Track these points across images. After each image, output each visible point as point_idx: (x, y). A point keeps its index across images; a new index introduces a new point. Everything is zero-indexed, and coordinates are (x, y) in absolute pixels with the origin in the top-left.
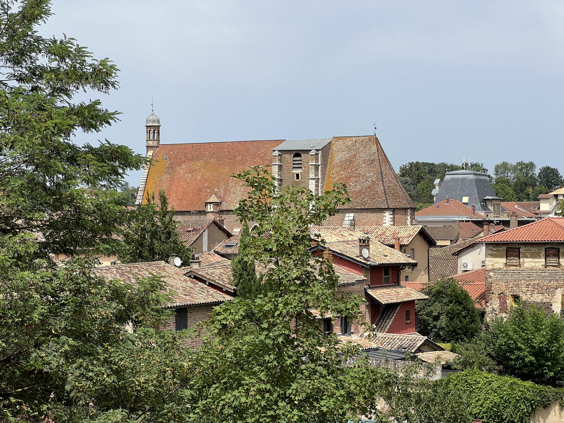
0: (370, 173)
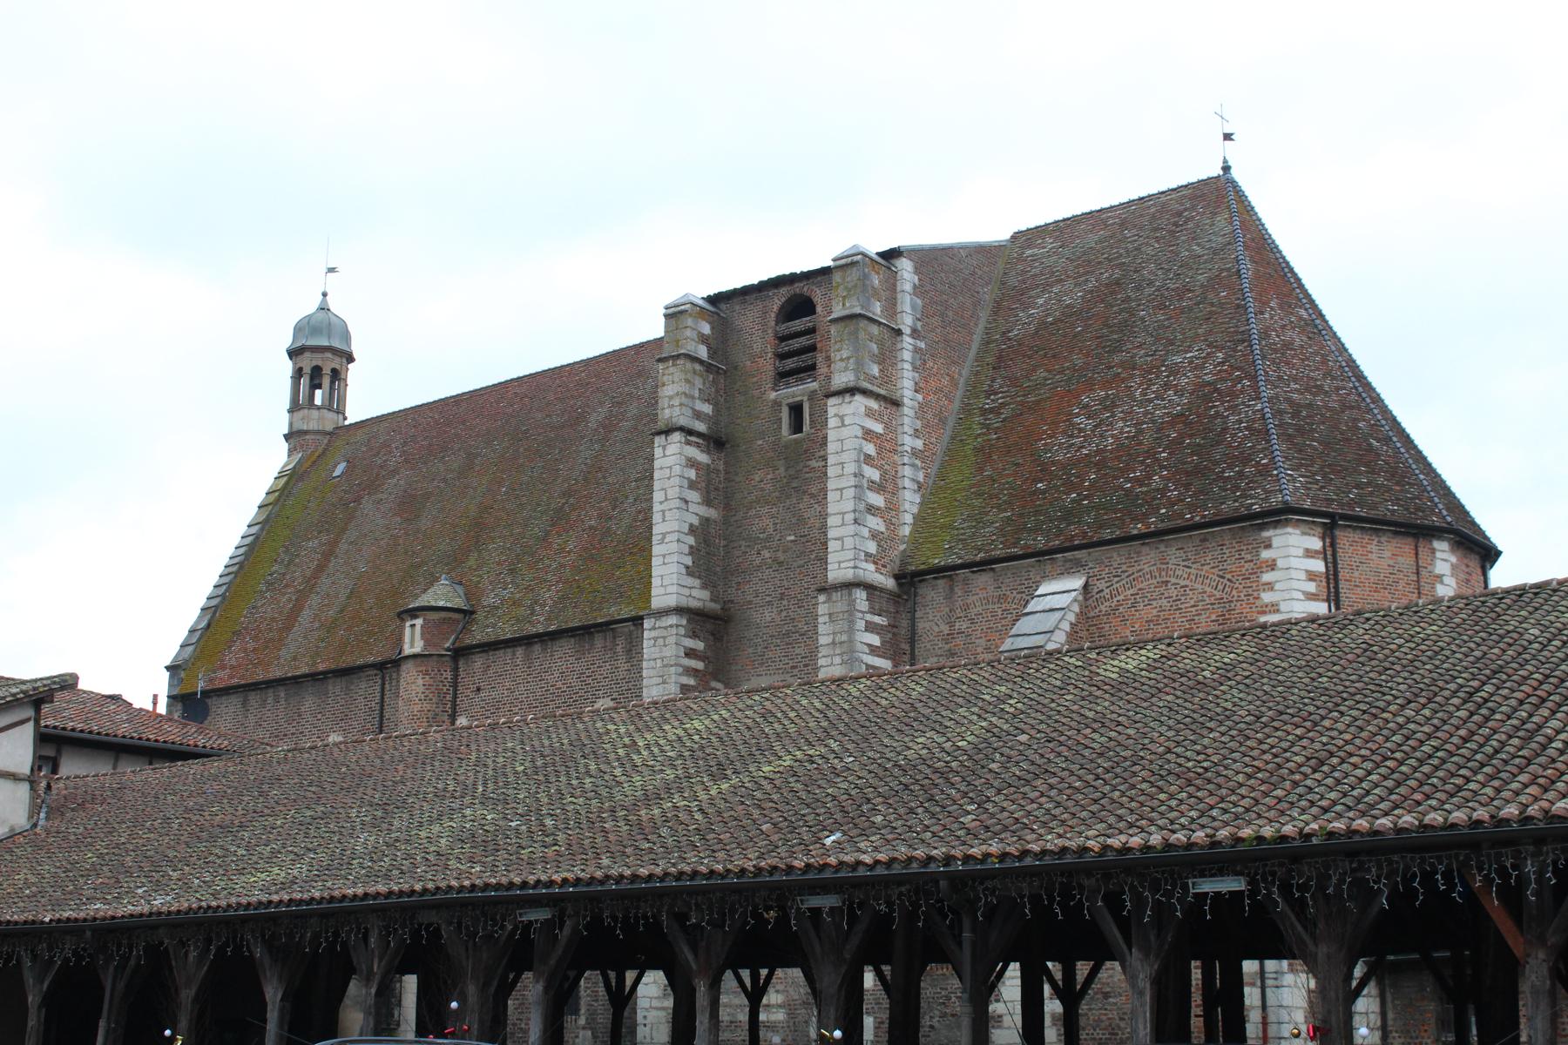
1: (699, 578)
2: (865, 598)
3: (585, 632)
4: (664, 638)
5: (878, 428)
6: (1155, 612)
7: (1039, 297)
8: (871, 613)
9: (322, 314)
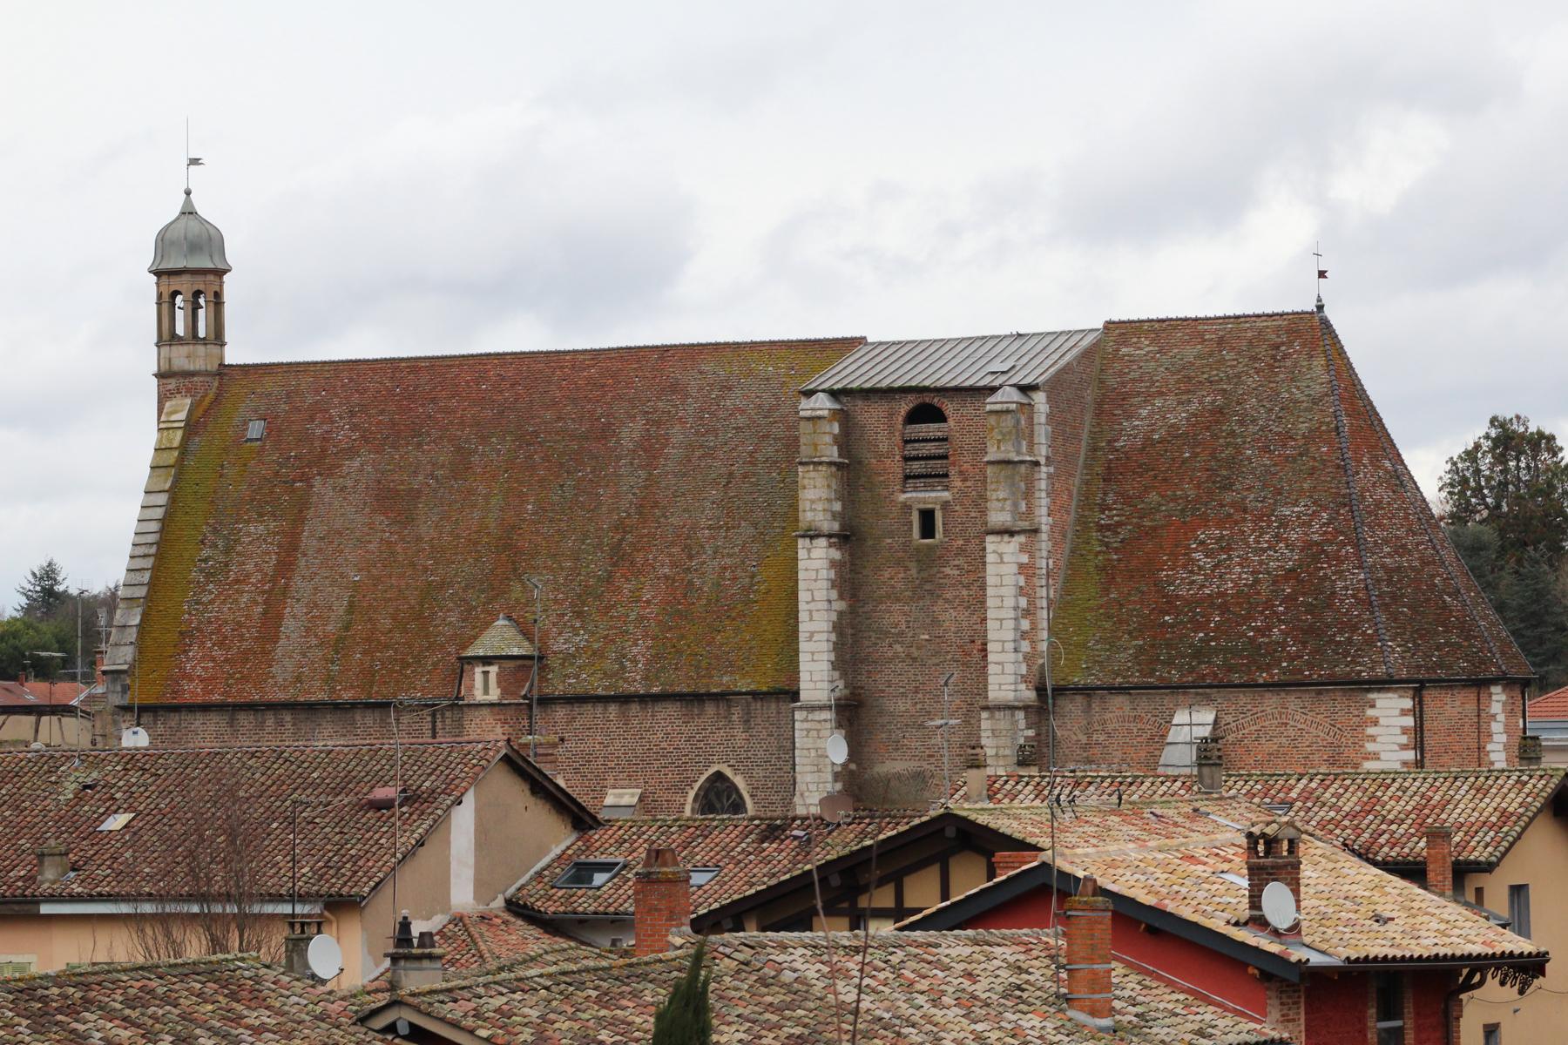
0: (1296, 504)
3: (694, 699)
4: (818, 730)
6: (1275, 747)
7: (1141, 407)
9: (192, 224)
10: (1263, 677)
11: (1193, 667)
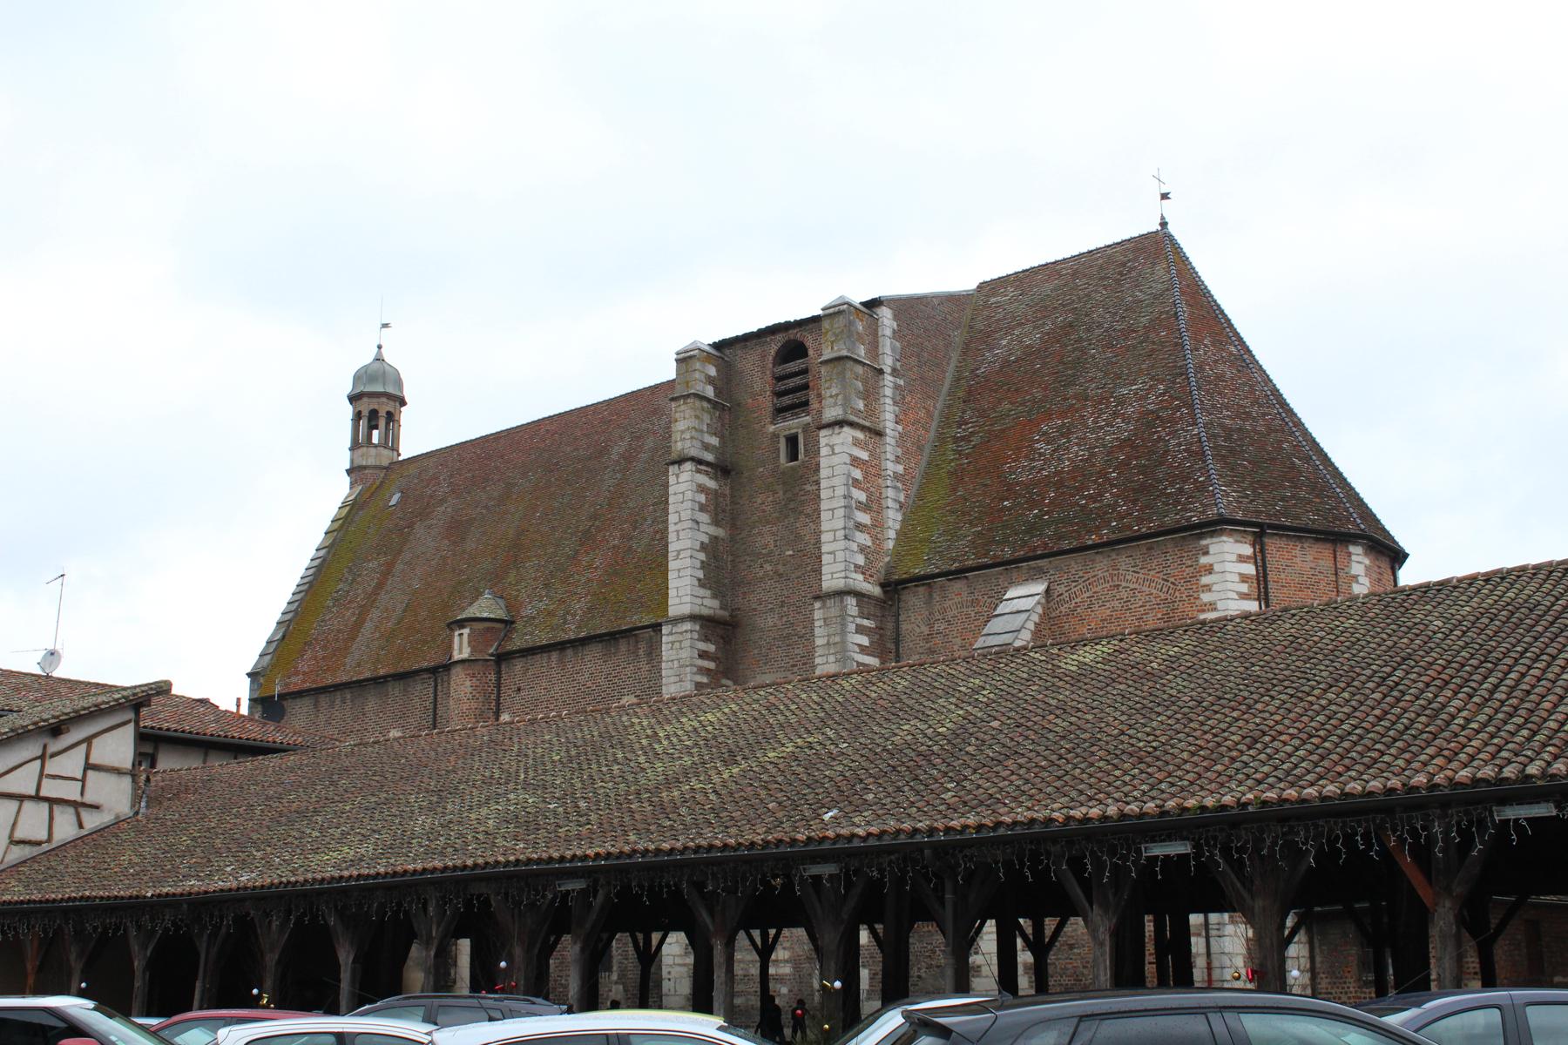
1: (710, 589)
2: (855, 604)
3: (611, 638)
4: (680, 642)
5: (864, 455)
6: (1108, 612)
7: (1002, 339)
8: (860, 617)
10: (1093, 539)
11: (1026, 542)
